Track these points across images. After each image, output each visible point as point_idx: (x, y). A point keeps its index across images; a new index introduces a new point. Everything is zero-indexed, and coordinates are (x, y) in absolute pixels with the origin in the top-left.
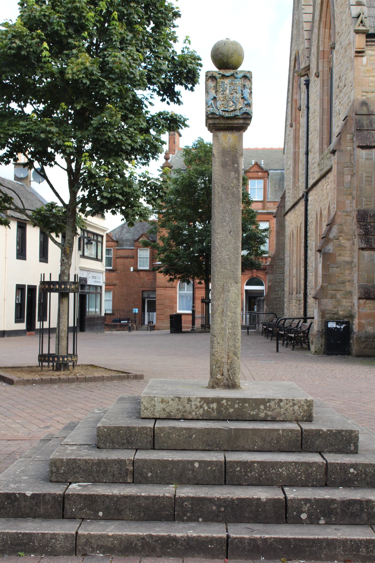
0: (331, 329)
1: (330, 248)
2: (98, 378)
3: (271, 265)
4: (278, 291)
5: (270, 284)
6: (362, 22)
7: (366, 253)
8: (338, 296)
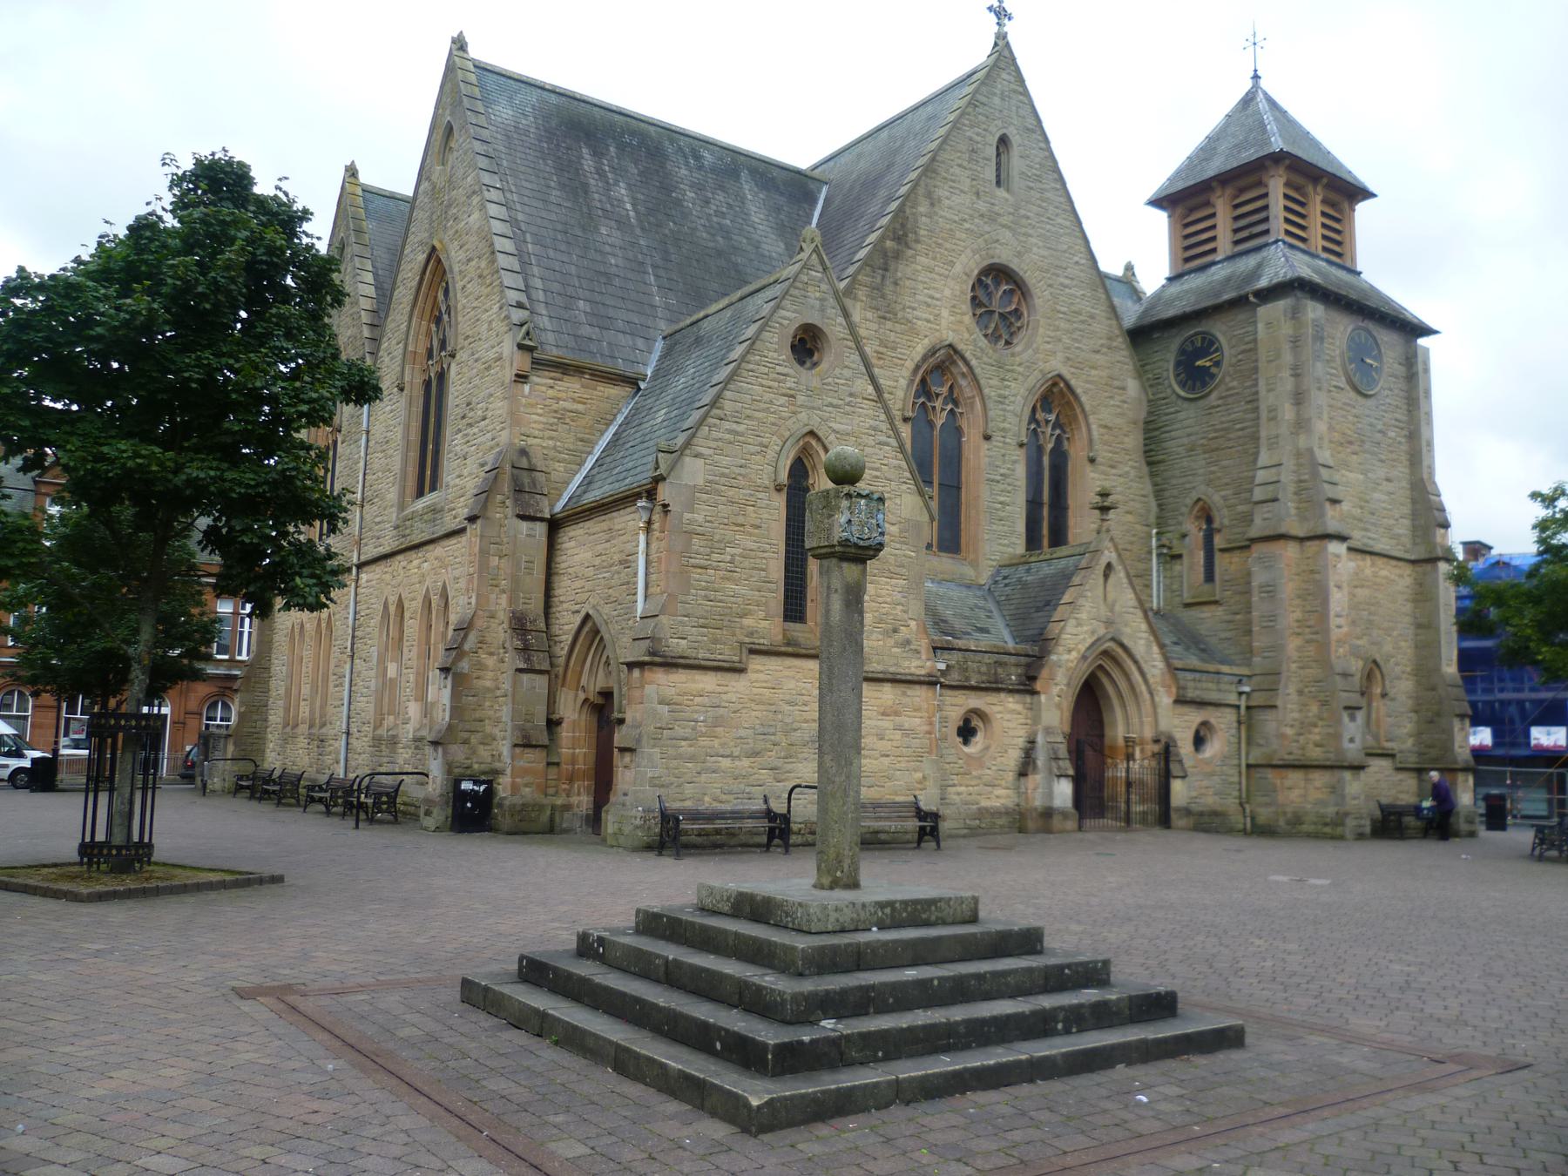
0: (465, 792)
1: (464, 666)
2: (136, 890)
3: (247, 678)
4: (256, 721)
5: (243, 709)
6: (528, 333)
7: (525, 677)
8: (473, 740)
